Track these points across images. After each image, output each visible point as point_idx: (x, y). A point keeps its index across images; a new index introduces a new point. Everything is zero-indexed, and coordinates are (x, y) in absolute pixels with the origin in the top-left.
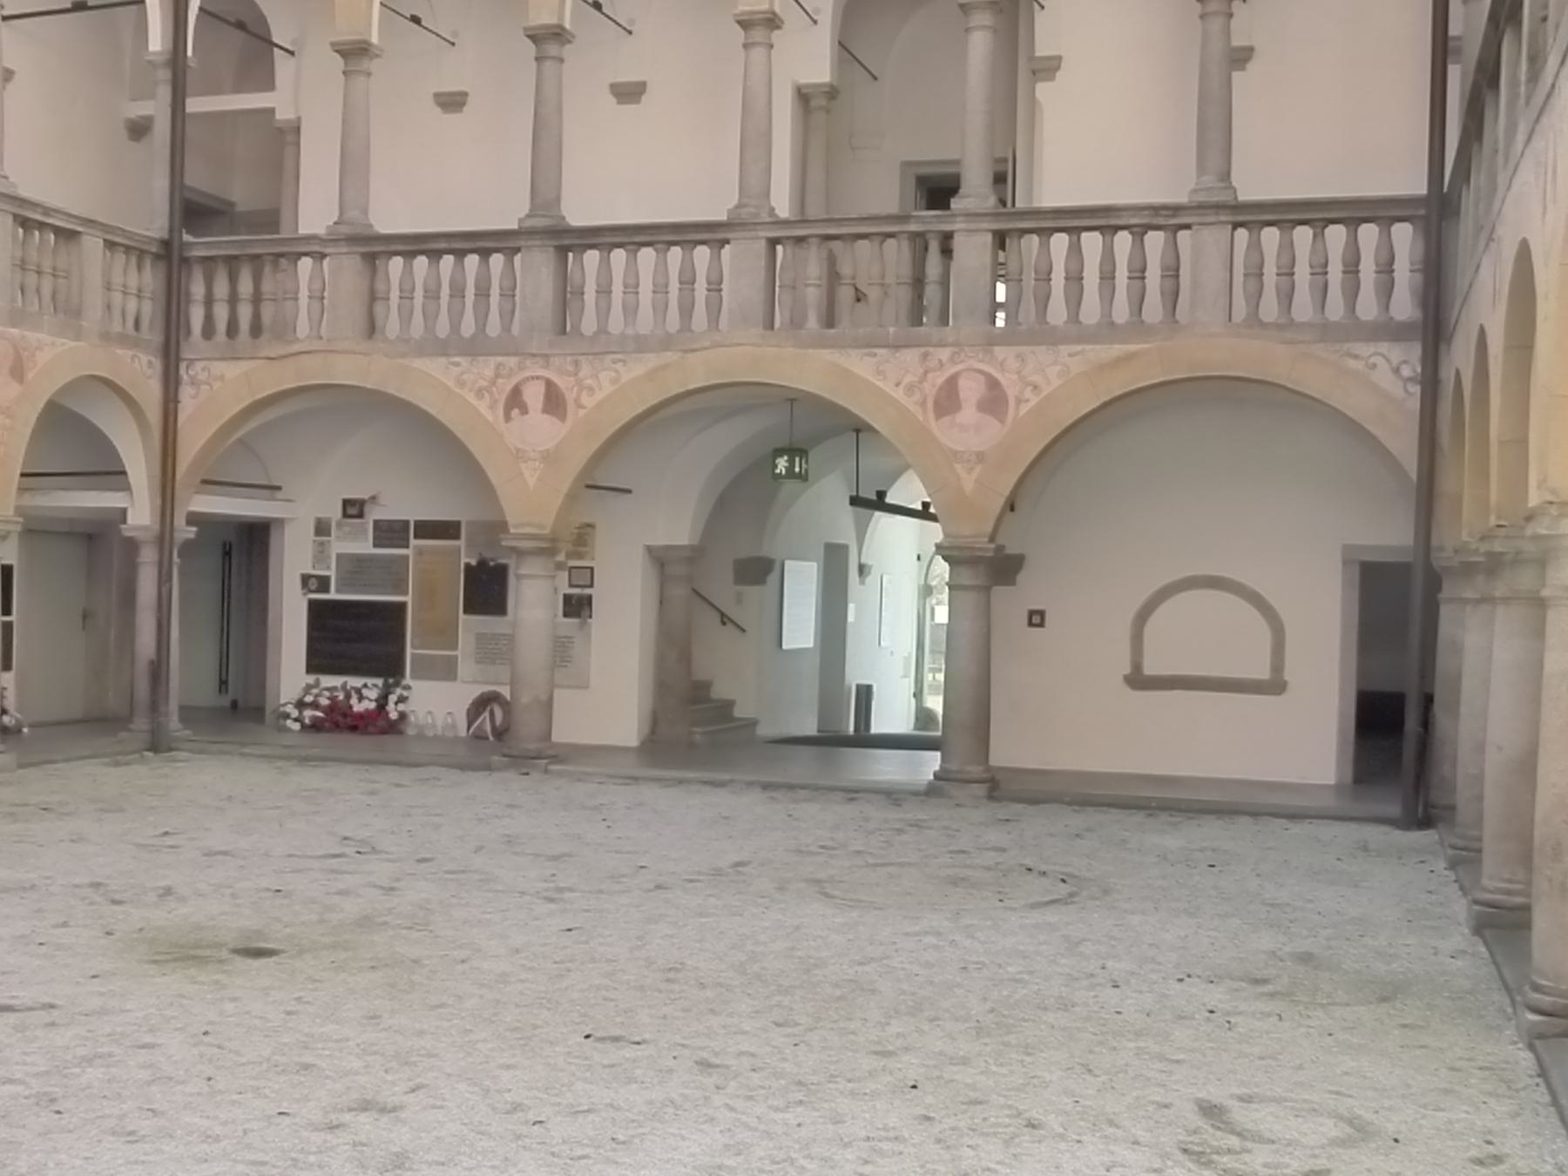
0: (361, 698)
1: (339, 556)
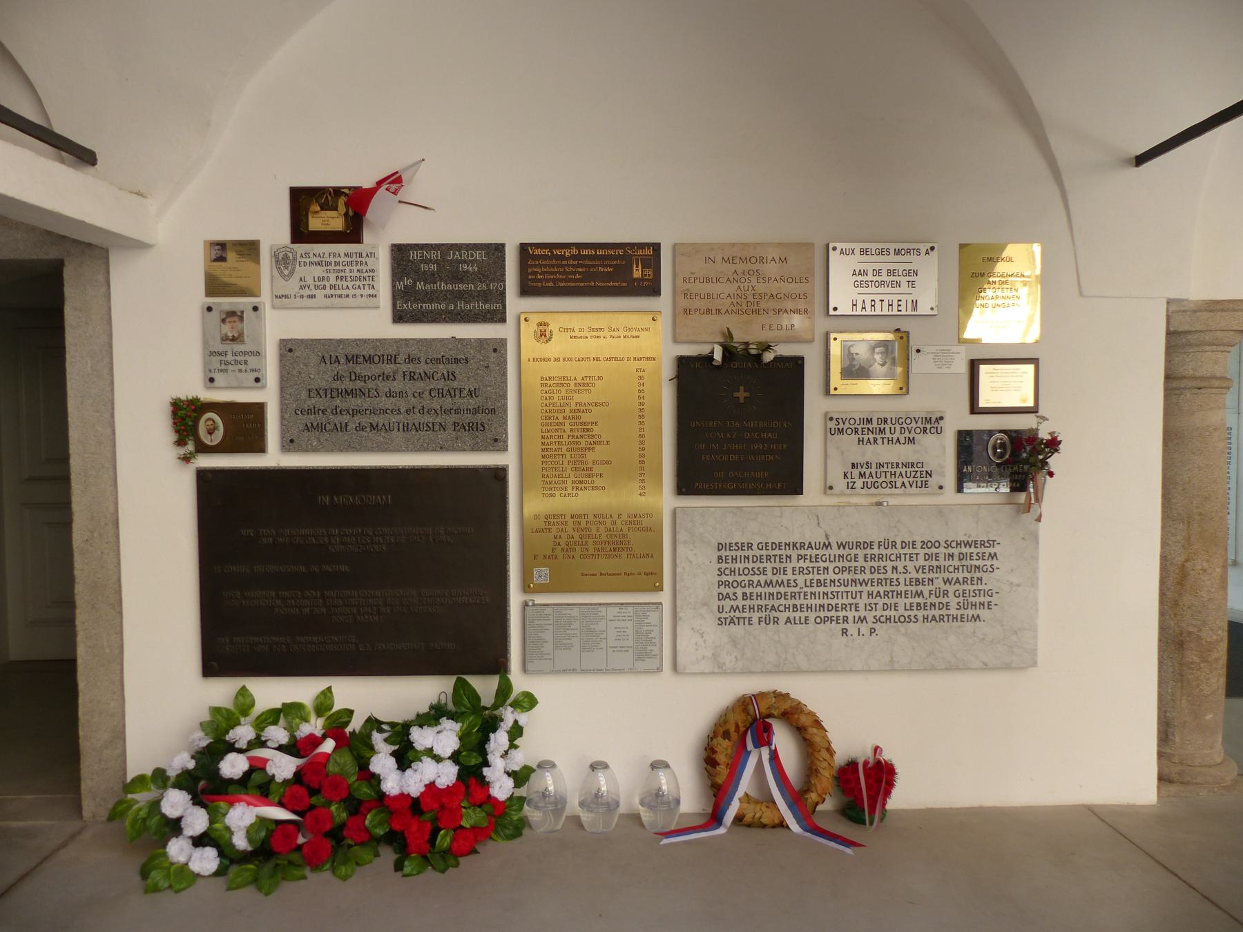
0: (405, 757)
1: (288, 348)
